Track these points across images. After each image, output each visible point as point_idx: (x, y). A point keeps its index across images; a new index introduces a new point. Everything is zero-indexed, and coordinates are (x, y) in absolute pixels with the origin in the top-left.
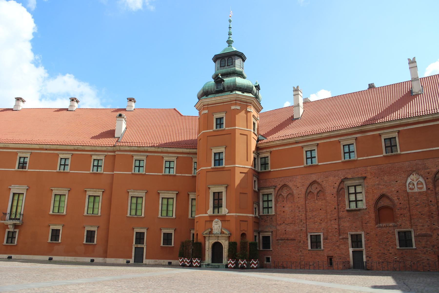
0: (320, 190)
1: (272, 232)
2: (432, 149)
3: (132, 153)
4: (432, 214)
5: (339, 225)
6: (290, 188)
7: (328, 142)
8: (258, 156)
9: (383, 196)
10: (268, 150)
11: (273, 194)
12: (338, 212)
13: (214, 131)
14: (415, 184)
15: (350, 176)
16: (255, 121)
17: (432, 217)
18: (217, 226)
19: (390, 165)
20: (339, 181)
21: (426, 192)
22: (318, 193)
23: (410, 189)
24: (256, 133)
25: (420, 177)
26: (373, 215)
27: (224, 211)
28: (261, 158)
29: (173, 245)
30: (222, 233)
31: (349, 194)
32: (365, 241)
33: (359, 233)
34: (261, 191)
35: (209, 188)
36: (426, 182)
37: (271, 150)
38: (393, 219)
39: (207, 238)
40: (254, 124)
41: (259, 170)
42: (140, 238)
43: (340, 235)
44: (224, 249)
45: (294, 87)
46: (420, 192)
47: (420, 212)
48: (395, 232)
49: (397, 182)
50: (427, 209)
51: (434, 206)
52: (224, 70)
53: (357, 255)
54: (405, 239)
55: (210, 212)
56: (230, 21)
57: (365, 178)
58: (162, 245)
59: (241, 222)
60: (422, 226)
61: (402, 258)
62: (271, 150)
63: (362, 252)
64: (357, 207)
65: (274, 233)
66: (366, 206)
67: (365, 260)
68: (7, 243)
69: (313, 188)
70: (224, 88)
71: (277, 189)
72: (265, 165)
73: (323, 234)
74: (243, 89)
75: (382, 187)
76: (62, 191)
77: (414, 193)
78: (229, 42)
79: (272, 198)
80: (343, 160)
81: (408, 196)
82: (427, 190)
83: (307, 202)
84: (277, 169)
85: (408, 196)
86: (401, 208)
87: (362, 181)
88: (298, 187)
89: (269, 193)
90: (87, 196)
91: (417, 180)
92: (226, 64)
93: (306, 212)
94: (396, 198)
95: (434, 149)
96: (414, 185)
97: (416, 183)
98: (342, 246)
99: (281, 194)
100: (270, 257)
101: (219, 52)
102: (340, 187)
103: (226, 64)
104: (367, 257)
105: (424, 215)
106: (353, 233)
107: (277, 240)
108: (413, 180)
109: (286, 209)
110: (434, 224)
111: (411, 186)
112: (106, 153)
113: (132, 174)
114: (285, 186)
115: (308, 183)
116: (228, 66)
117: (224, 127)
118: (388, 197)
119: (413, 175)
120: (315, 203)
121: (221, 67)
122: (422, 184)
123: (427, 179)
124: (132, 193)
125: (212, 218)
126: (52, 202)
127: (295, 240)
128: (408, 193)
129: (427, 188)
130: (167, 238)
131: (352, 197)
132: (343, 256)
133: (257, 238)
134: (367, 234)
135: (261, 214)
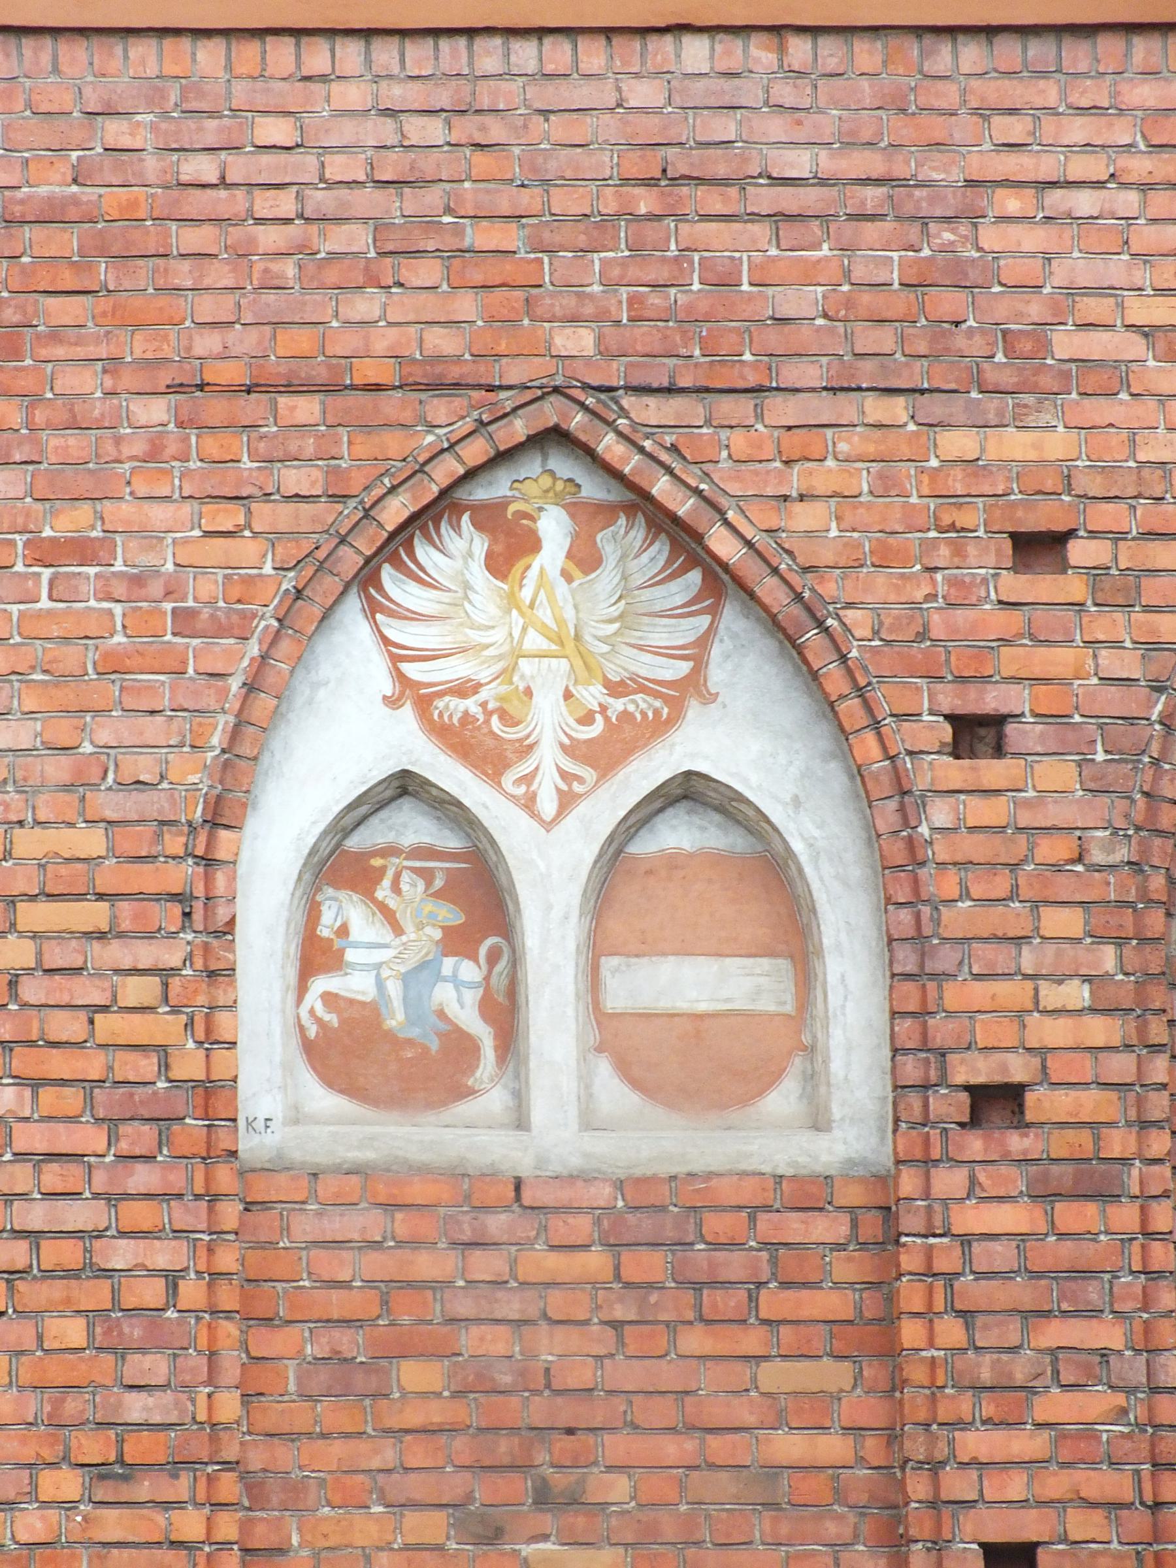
21: (881, 1217)
25: (744, 667)
36: (901, 868)
46: (656, 1218)
123: (976, 733)
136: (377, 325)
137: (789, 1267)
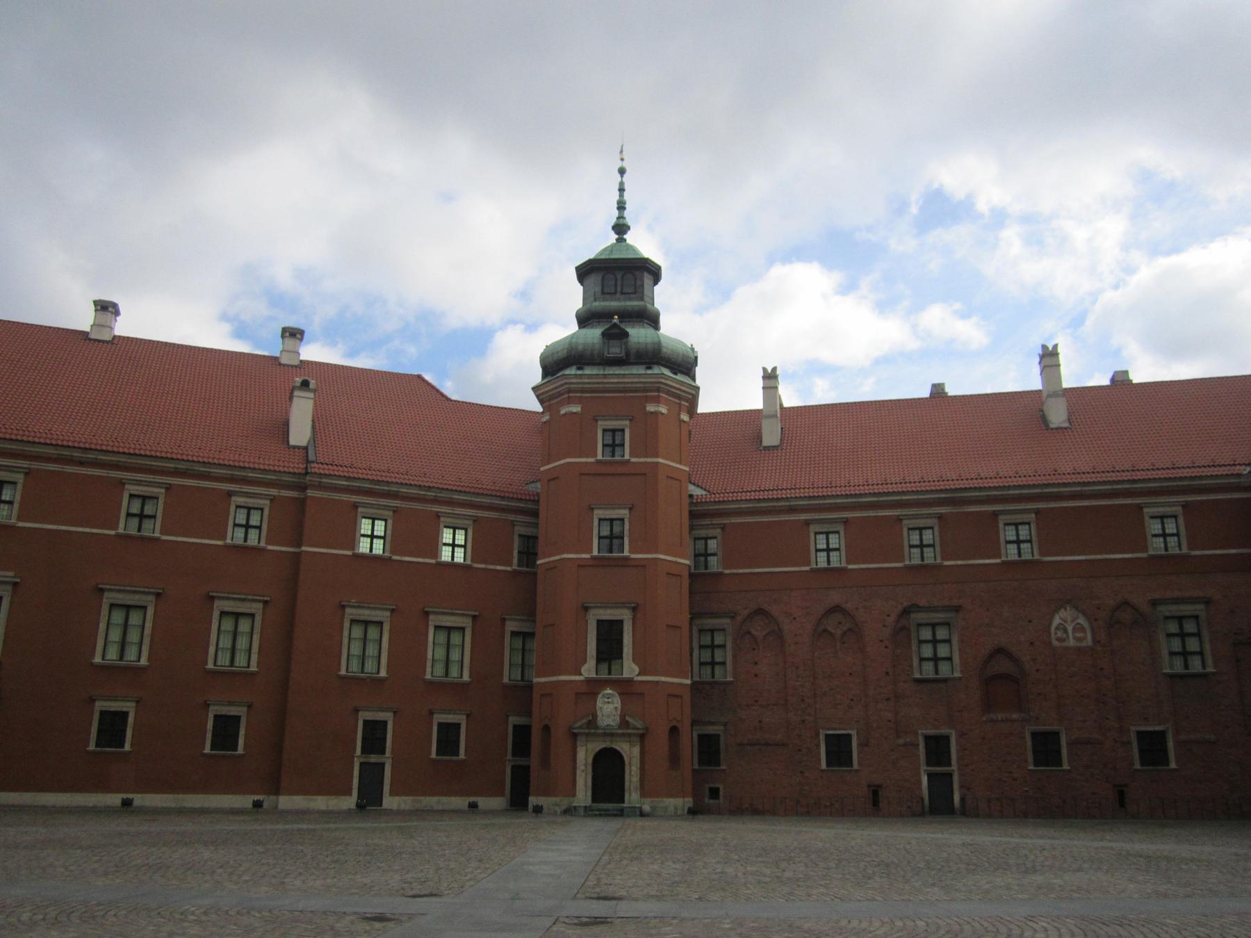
7: (873, 520)
9: (1000, 651)
13: (598, 462)
14: (1070, 629)
15: (923, 602)
18: (608, 708)
20: (900, 608)
22: (844, 634)
23: (1058, 639)
25: (1081, 615)
27: (629, 669)
29: (462, 755)
30: (624, 723)
32: (958, 752)
33: (944, 731)
35: (586, 609)
37: (726, 521)
44: (627, 768)
45: (765, 370)
53: (941, 783)
54: (1046, 748)
55: (589, 670)
56: (622, 171)
57: (958, 609)
58: (434, 756)
62: (726, 521)
63: (950, 775)
70: (628, 354)
73: (858, 733)
74: (675, 363)
76: (137, 597)
77: (1067, 648)
78: (621, 228)
84: (741, 571)
87: (949, 615)
90: (216, 614)
91: (1073, 621)
92: (619, 289)
96: (1065, 631)
97: (1069, 627)
99: (749, 633)
103: (619, 289)
104: (962, 787)
106: (932, 732)
107: (739, 745)
111: (1060, 634)
116: (622, 293)
117: (627, 457)
121: (603, 293)
122: (1083, 629)
124: (354, 611)
125: (593, 688)
126: (102, 626)
129: (1094, 639)
130: (449, 735)
134: (961, 735)
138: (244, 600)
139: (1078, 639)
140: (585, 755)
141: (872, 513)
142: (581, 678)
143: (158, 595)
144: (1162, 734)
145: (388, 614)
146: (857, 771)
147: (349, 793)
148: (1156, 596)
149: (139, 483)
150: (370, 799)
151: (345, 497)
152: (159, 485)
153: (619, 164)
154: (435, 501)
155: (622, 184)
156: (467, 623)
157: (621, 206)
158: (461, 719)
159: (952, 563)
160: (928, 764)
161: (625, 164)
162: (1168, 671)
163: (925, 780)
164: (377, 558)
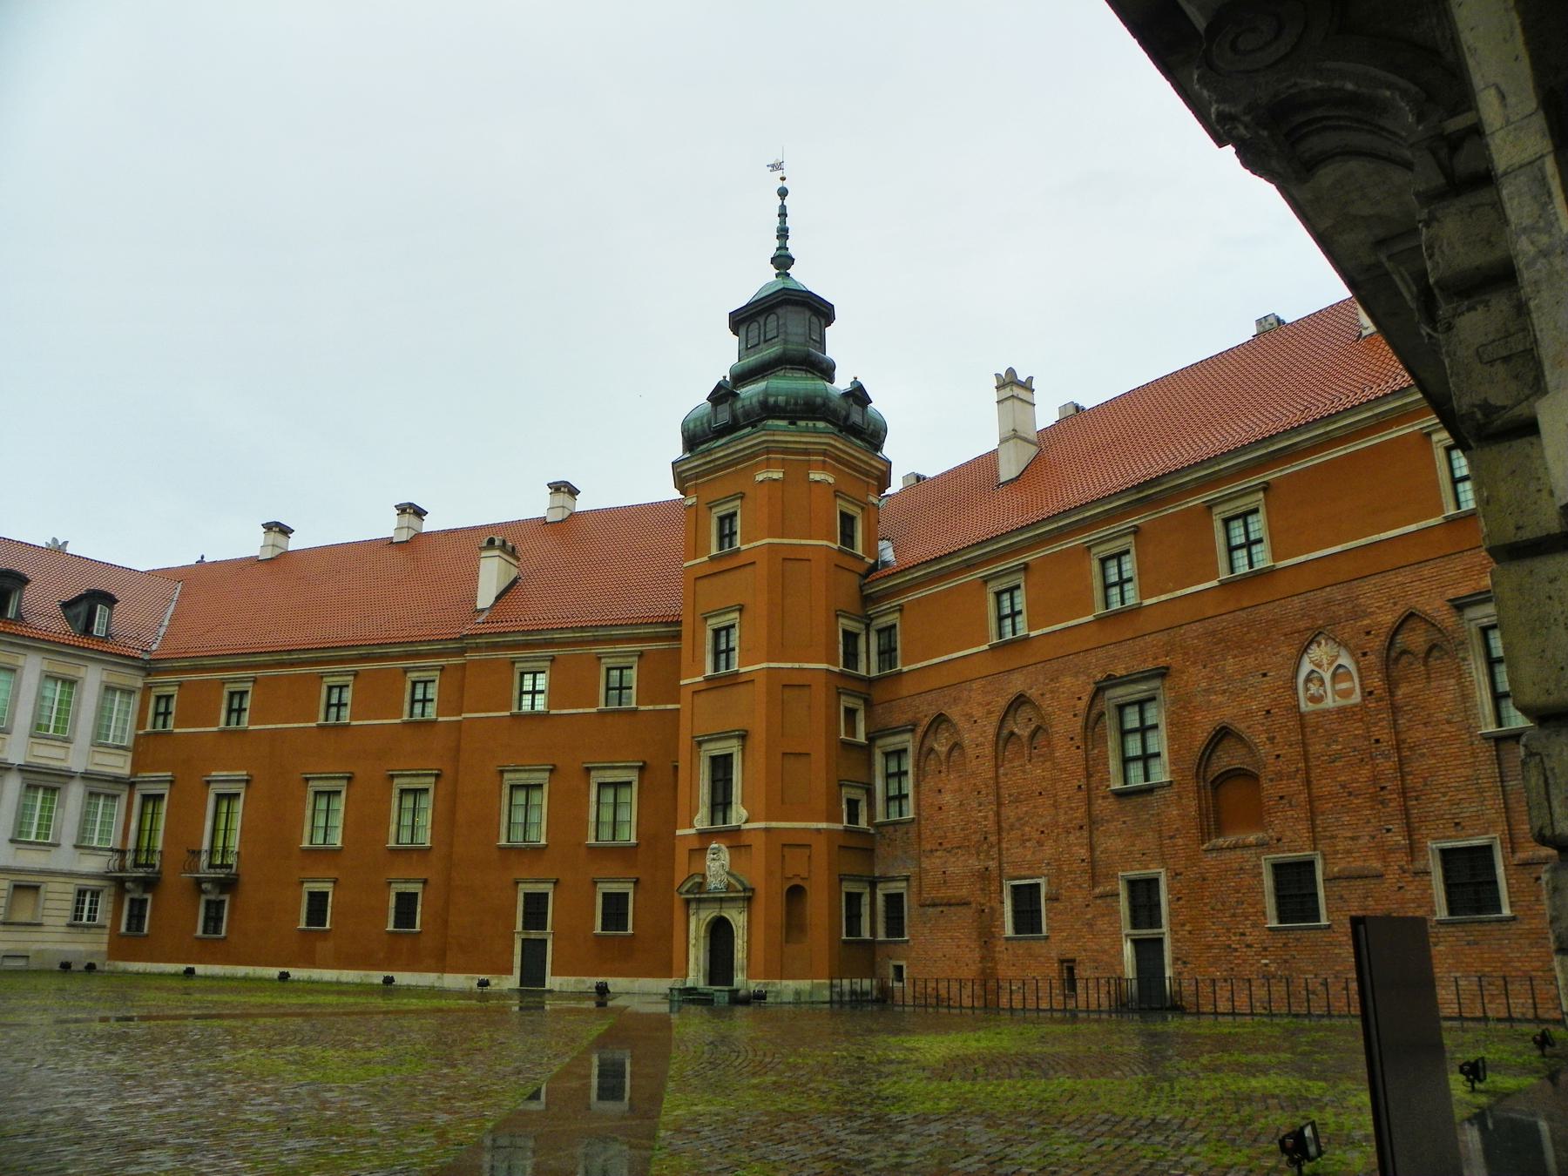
0: (1038, 728)
1: (907, 879)
2: (1376, 538)
3: (511, 654)
4: (1383, 788)
5: (1092, 849)
6: (954, 725)
8: (868, 627)
9: (1223, 734)
10: (896, 602)
11: (910, 749)
12: (1089, 803)
13: (712, 559)
15: (1120, 671)
16: (852, 510)
17: (1382, 803)
18: (717, 865)
19: (1243, 614)
20: (1091, 688)
22: (1033, 735)
23: (1314, 699)
24: (859, 551)
25: (1343, 652)
26: (1192, 805)
27: (738, 814)
28: (879, 631)
30: (729, 887)
31: (1124, 733)
32: (1170, 903)
34: (880, 742)
36: (1359, 670)
38: (1257, 818)
39: (693, 906)
40: (848, 520)
41: (874, 673)
42: (535, 909)
43: (1094, 884)
46: (1341, 710)
47: (1343, 787)
48: (1259, 866)
49: (1265, 675)
50: (1366, 771)
51: (1387, 758)
52: (753, 359)
55: (702, 821)
56: (783, 193)
57: (1162, 673)
59: (786, 850)
60: (1352, 839)
61: (1286, 961)
63: (1160, 941)
64: (1147, 778)
65: (914, 883)
66: (1172, 772)
67: (1168, 973)
68: (205, 931)
69: (1019, 720)
70: (734, 417)
71: (920, 730)
72: (887, 654)
73: (1049, 883)
75: (1220, 698)
76: (333, 782)
77: (1328, 711)
78: (783, 261)
79: (909, 764)
80: (1100, 611)
81: (1303, 726)
82: (1364, 699)
83: (1001, 771)
84: (919, 665)
85: (1303, 726)
86: (1280, 776)
87: (1155, 683)
88: (976, 723)
89: (900, 747)
90: (396, 793)
91: (1330, 664)
93: (1000, 805)
94: (1263, 737)
95: (1383, 536)
97: (1328, 677)
98: (1102, 924)
99: (932, 750)
100: (903, 963)
101: (742, 302)
102: (1095, 711)
104: (1176, 960)
105: (1356, 796)
106: (1134, 874)
108: (1320, 666)
109: (947, 797)
110: (1388, 830)
111: (1313, 688)
112: (443, 661)
113: (512, 715)
114: (940, 720)
115: (1002, 702)
118: (1240, 738)
119: (1319, 644)
120: (1024, 772)
123: (1365, 654)
126: (309, 813)
127: (967, 904)
128: (1302, 716)
130: (615, 908)
131: (1134, 746)
132: (1105, 958)
133: (866, 900)
135: (880, 819)
136: (1302, 625)
137: (1355, 713)
138: (417, 775)
139: (1347, 694)
140: (698, 924)
141: (1056, 548)
142: (693, 831)
143: (349, 779)
144: (1488, 849)
145: (547, 775)
146: (1047, 938)
147: (510, 971)
148: (1463, 590)
149: (333, 674)
150: (533, 974)
151: (501, 655)
152: (347, 673)
153: (780, 184)
154: (596, 641)
155: (783, 207)
156: (633, 776)
157: (783, 234)
158: (628, 888)
159: (1154, 600)
160: (1135, 925)
161: (786, 184)
162: (1492, 728)
163: (1128, 949)
164: (540, 715)
